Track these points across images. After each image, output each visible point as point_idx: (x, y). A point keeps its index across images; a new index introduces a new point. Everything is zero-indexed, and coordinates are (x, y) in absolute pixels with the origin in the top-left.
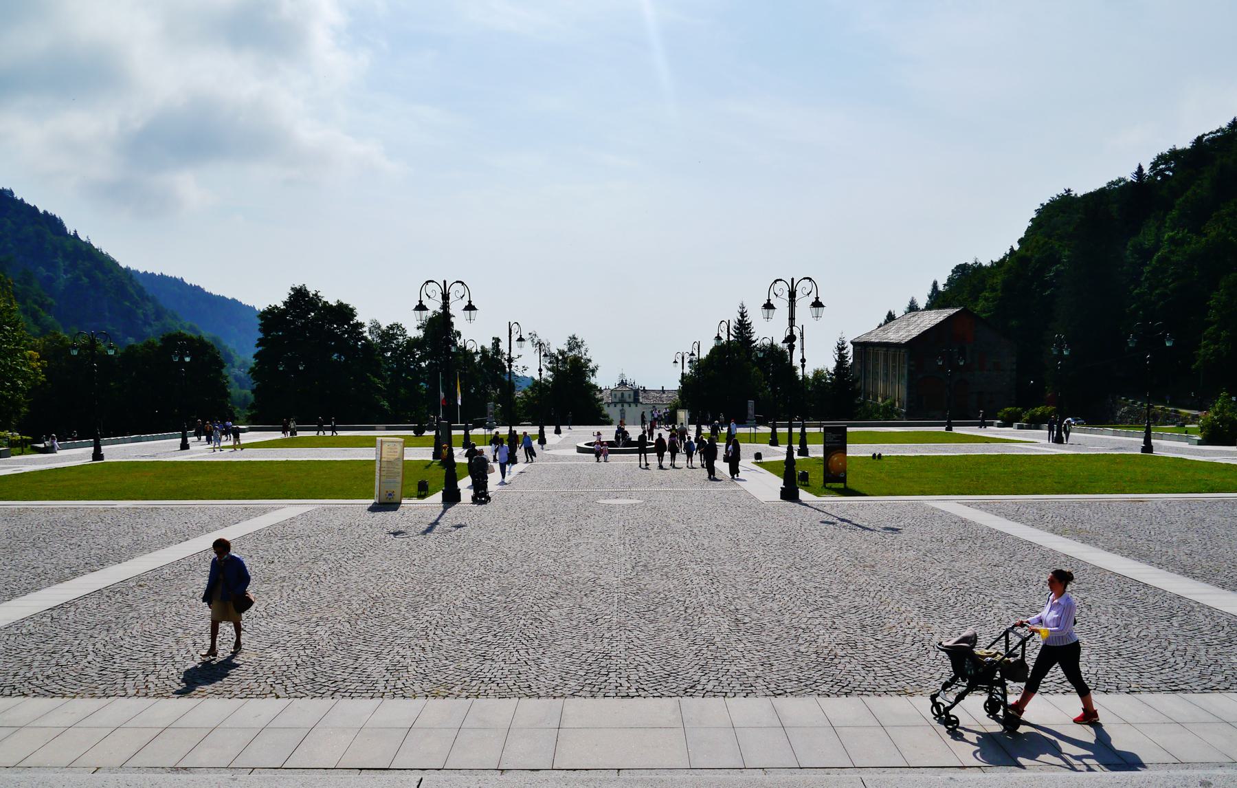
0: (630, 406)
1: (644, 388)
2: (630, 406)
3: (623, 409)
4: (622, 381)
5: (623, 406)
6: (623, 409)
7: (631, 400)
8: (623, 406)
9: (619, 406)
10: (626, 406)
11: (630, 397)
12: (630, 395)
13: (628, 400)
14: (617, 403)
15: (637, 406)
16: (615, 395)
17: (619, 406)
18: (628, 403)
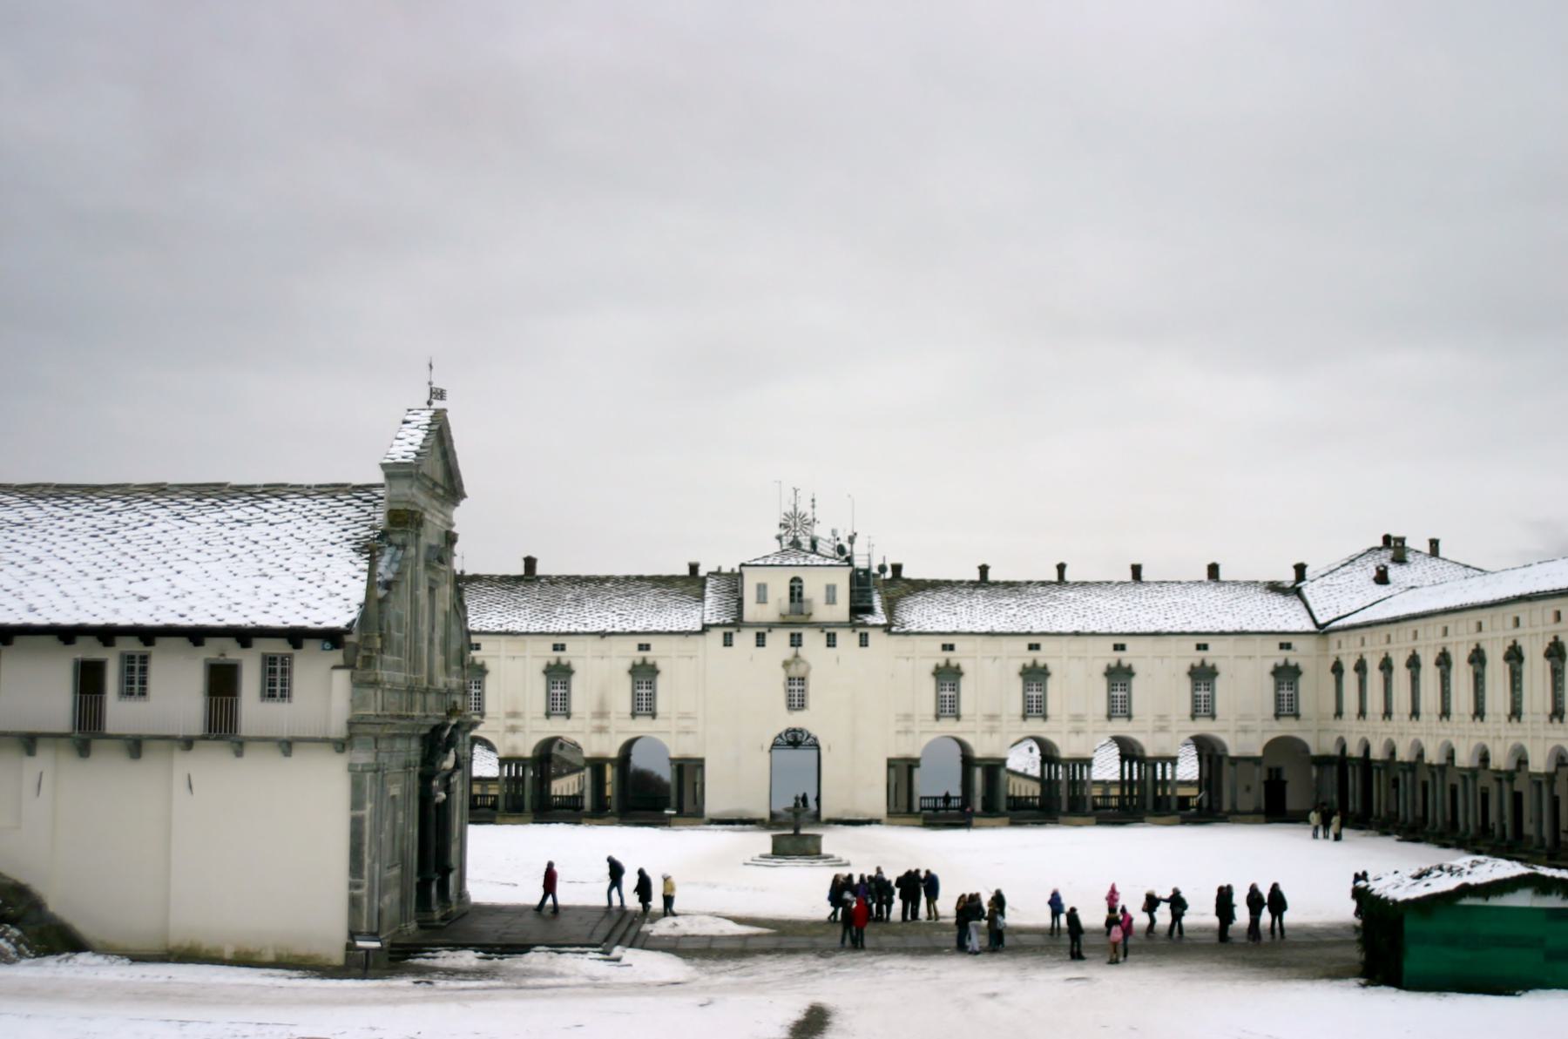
0: (831, 641)
1: (897, 569)
2: (831, 641)
3: (797, 656)
4: (796, 544)
5: (796, 641)
6: (797, 656)
7: (841, 610)
8: (796, 641)
9: (779, 641)
10: (813, 641)
11: (831, 599)
12: (831, 591)
13: (822, 613)
14: (771, 626)
15: (864, 641)
16: (762, 589)
17: (779, 641)
18: (821, 626)
